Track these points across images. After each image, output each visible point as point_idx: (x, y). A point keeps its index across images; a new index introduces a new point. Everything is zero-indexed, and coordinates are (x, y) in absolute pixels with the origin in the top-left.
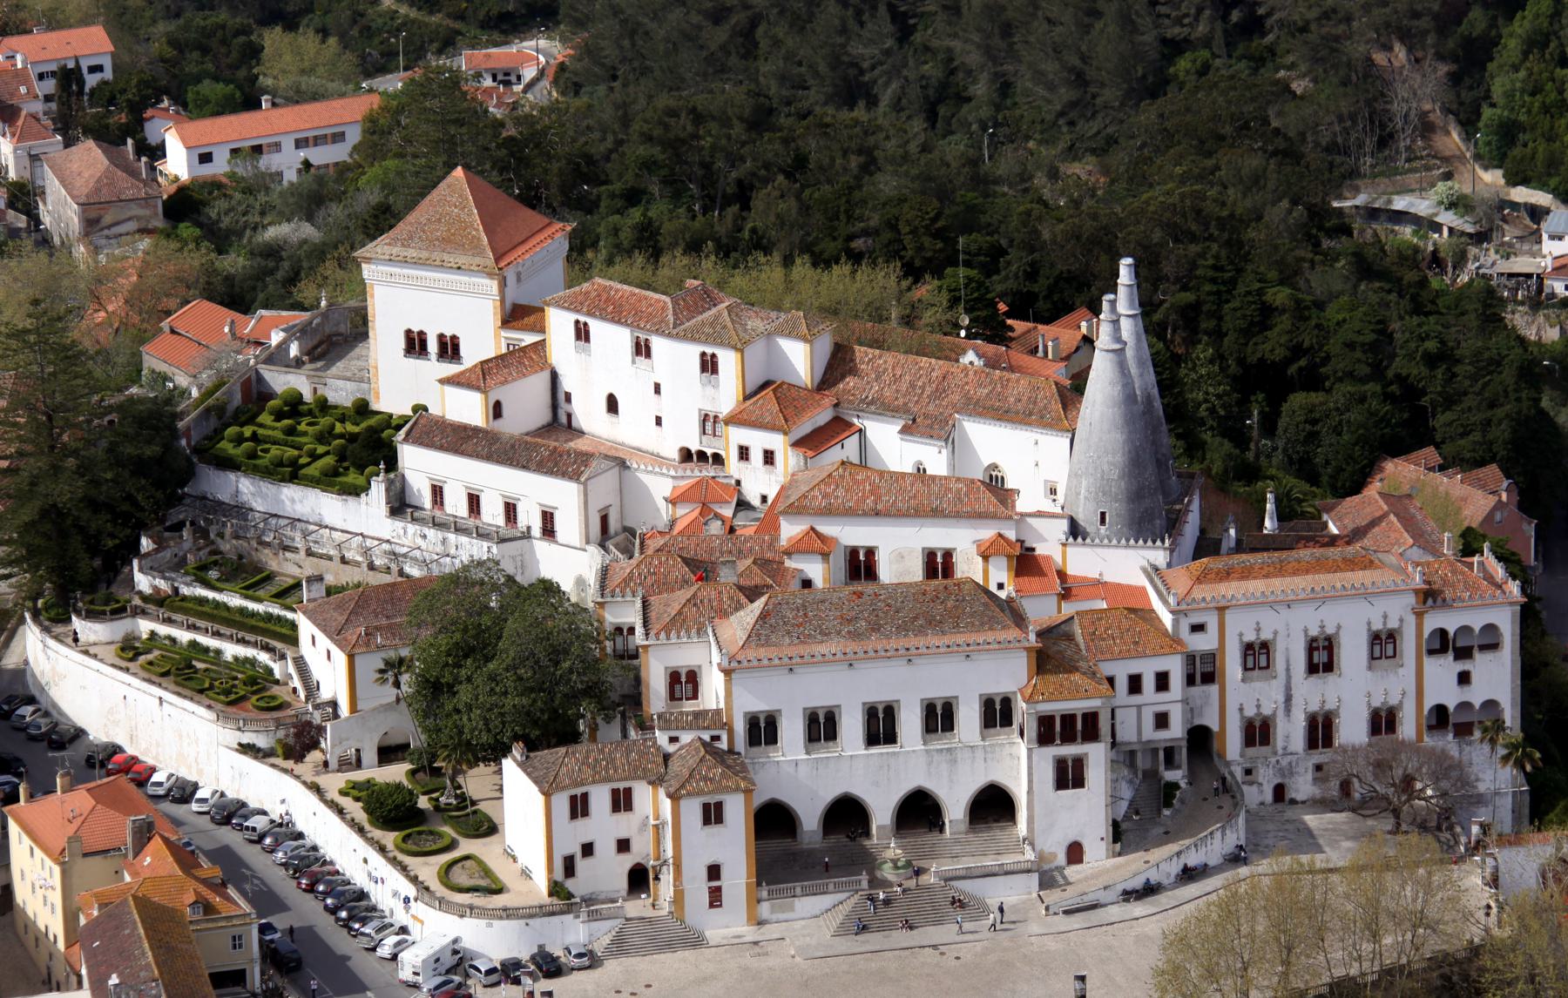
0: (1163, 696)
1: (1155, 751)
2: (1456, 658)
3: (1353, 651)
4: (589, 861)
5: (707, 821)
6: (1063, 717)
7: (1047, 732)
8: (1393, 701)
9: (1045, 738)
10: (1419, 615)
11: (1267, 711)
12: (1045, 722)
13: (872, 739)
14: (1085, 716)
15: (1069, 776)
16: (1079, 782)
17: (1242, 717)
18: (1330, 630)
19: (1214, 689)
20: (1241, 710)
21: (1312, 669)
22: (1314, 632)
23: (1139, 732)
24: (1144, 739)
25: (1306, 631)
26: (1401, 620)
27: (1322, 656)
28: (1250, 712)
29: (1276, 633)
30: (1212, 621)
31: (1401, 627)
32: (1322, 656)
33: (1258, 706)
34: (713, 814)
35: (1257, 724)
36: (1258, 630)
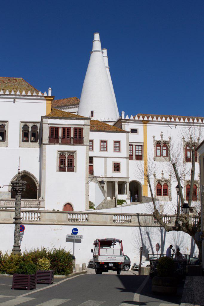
1: (113, 183)
6: (64, 129)
7: (55, 136)
11: (167, 177)
12: (54, 131)
14: (75, 129)
15: (67, 164)
19: (141, 163)
23: (106, 172)
24: (107, 177)
25: (184, 139)
28: (159, 177)
29: (170, 138)
30: (139, 127)
33: (163, 174)
35: (163, 184)
36: (162, 136)
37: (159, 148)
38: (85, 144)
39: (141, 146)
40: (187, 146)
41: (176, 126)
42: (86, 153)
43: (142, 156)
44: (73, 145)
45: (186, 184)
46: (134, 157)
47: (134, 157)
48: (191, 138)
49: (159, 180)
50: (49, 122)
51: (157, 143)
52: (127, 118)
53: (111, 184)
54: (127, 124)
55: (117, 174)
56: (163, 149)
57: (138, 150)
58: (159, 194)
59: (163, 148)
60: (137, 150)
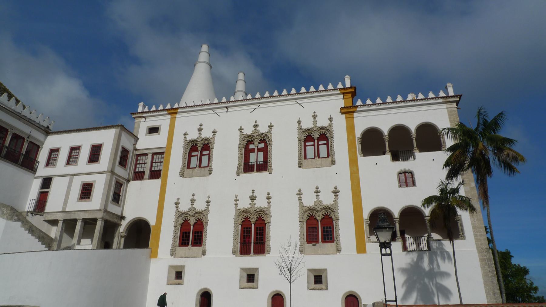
0: (94, 167)
1: (75, 221)
2: (395, 158)
3: (285, 148)
8: (327, 200)
10: (348, 111)
11: (200, 206)
18: (263, 129)
19: (157, 182)
20: (177, 204)
22: (249, 130)
24: (67, 210)
25: (241, 129)
26: (331, 119)
27: (255, 154)
28: (185, 207)
31: (330, 125)
32: (255, 154)
33: (193, 201)
35: (192, 221)
36: (200, 130)
39: (162, 153)
40: (250, 142)
41: (230, 109)
43: (161, 170)
45: (241, 217)
46: (147, 174)
47: (147, 174)
48: (256, 126)
52: (146, 110)
53: (69, 225)
54: (143, 120)
55: (85, 205)
56: (201, 155)
57: (158, 162)
58: (185, 244)
59: (204, 153)
60: (155, 162)
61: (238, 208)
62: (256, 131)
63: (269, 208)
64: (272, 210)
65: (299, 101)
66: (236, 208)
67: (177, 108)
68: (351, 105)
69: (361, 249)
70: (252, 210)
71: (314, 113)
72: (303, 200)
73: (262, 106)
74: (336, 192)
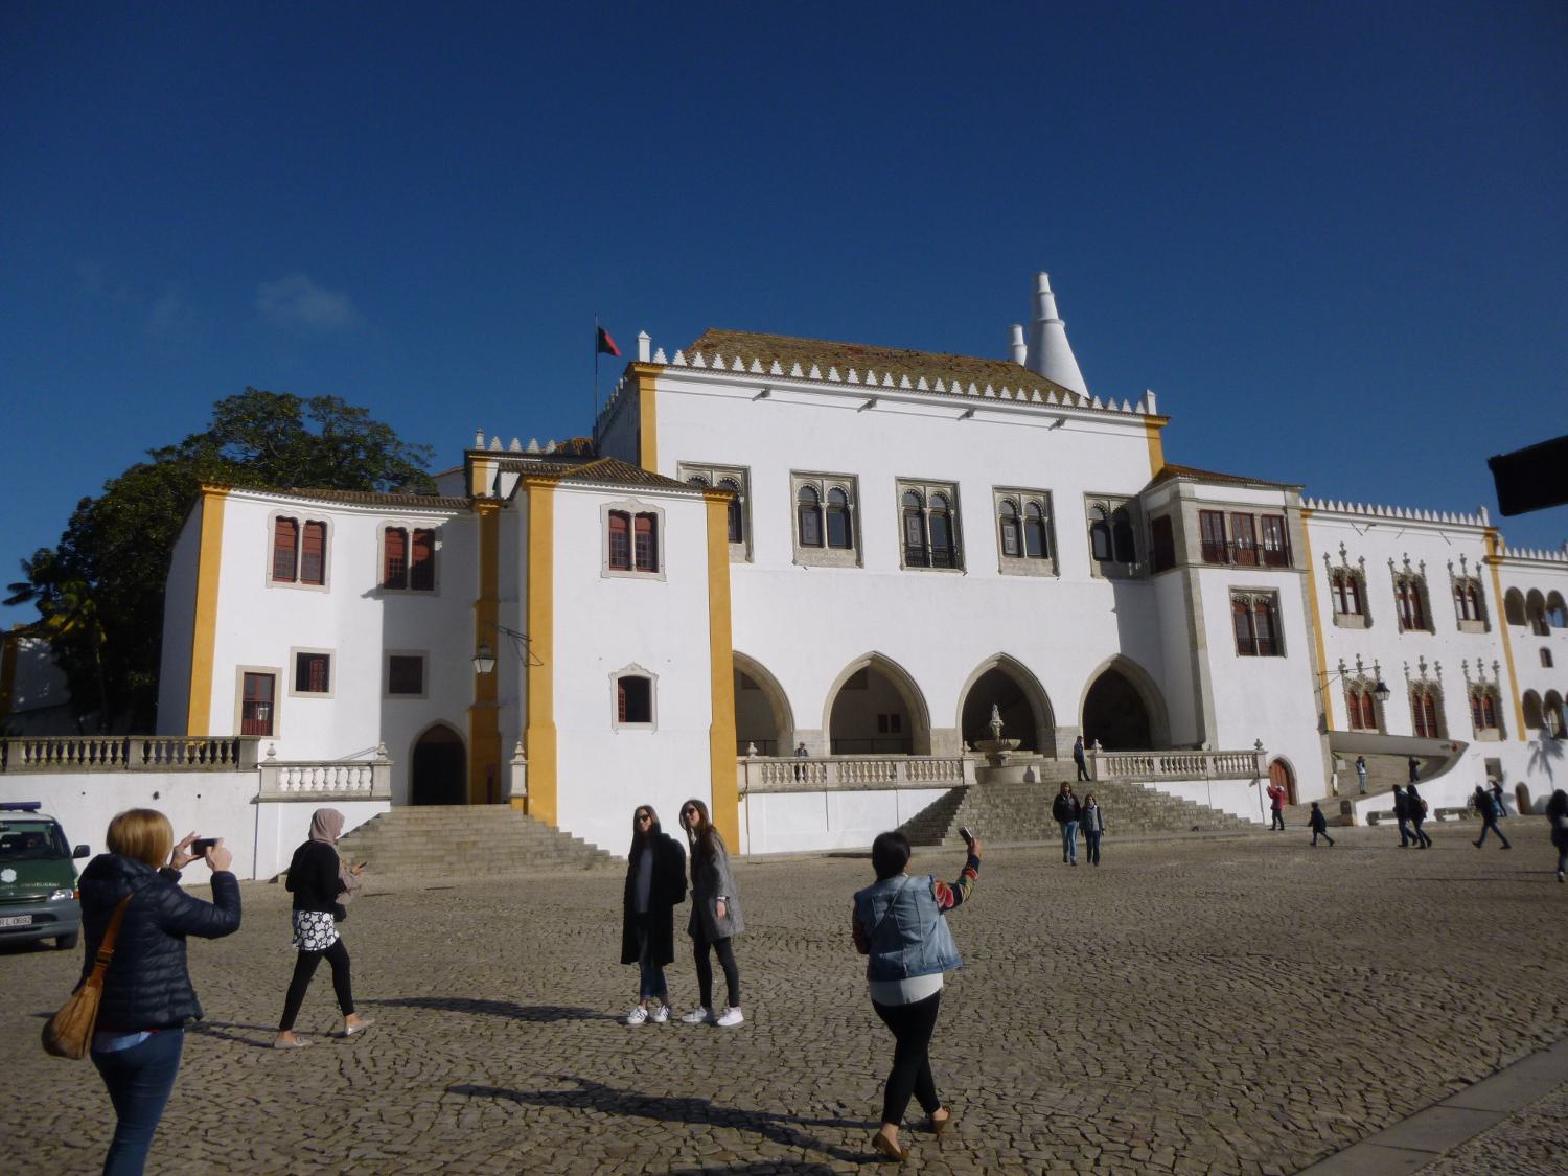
2: (1536, 633)
3: (1442, 604)
4: (312, 701)
5: (619, 559)
8: (1490, 678)
9: (1215, 554)
10: (1491, 560)
13: (916, 557)
16: (1273, 645)
17: (1346, 681)
21: (1406, 623)
22: (1400, 568)
25: (1391, 564)
26: (1479, 568)
29: (1362, 561)
34: (634, 546)
35: (1361, 694)
36: (1343, 553)
37: (1337, 589)
38: (1297, 565)
41: (1371, 528)
42: (1303, 597)
44: (1264, 569)
48: (1407, 562)
49: (1355, 683)
50: (1197, 495)
51: (1334, 577)
61: (1410, 679)
62: (1410, 571)
63: (1439, 683)
64: (1443, 684)
65: (1446, 534)
66: (1407, 679)
67: (1311, 511)
68: (1492, 554)
69: (1522, 737)
70: (1426, 684)
71: (1462, 555)
72: (1469, 675)
73: (1407, 530)
74: (1496, 667)
